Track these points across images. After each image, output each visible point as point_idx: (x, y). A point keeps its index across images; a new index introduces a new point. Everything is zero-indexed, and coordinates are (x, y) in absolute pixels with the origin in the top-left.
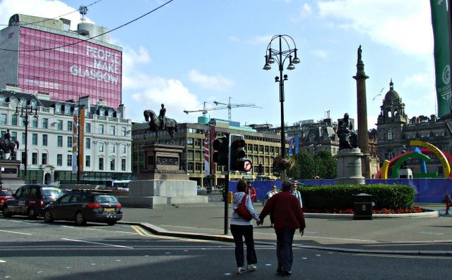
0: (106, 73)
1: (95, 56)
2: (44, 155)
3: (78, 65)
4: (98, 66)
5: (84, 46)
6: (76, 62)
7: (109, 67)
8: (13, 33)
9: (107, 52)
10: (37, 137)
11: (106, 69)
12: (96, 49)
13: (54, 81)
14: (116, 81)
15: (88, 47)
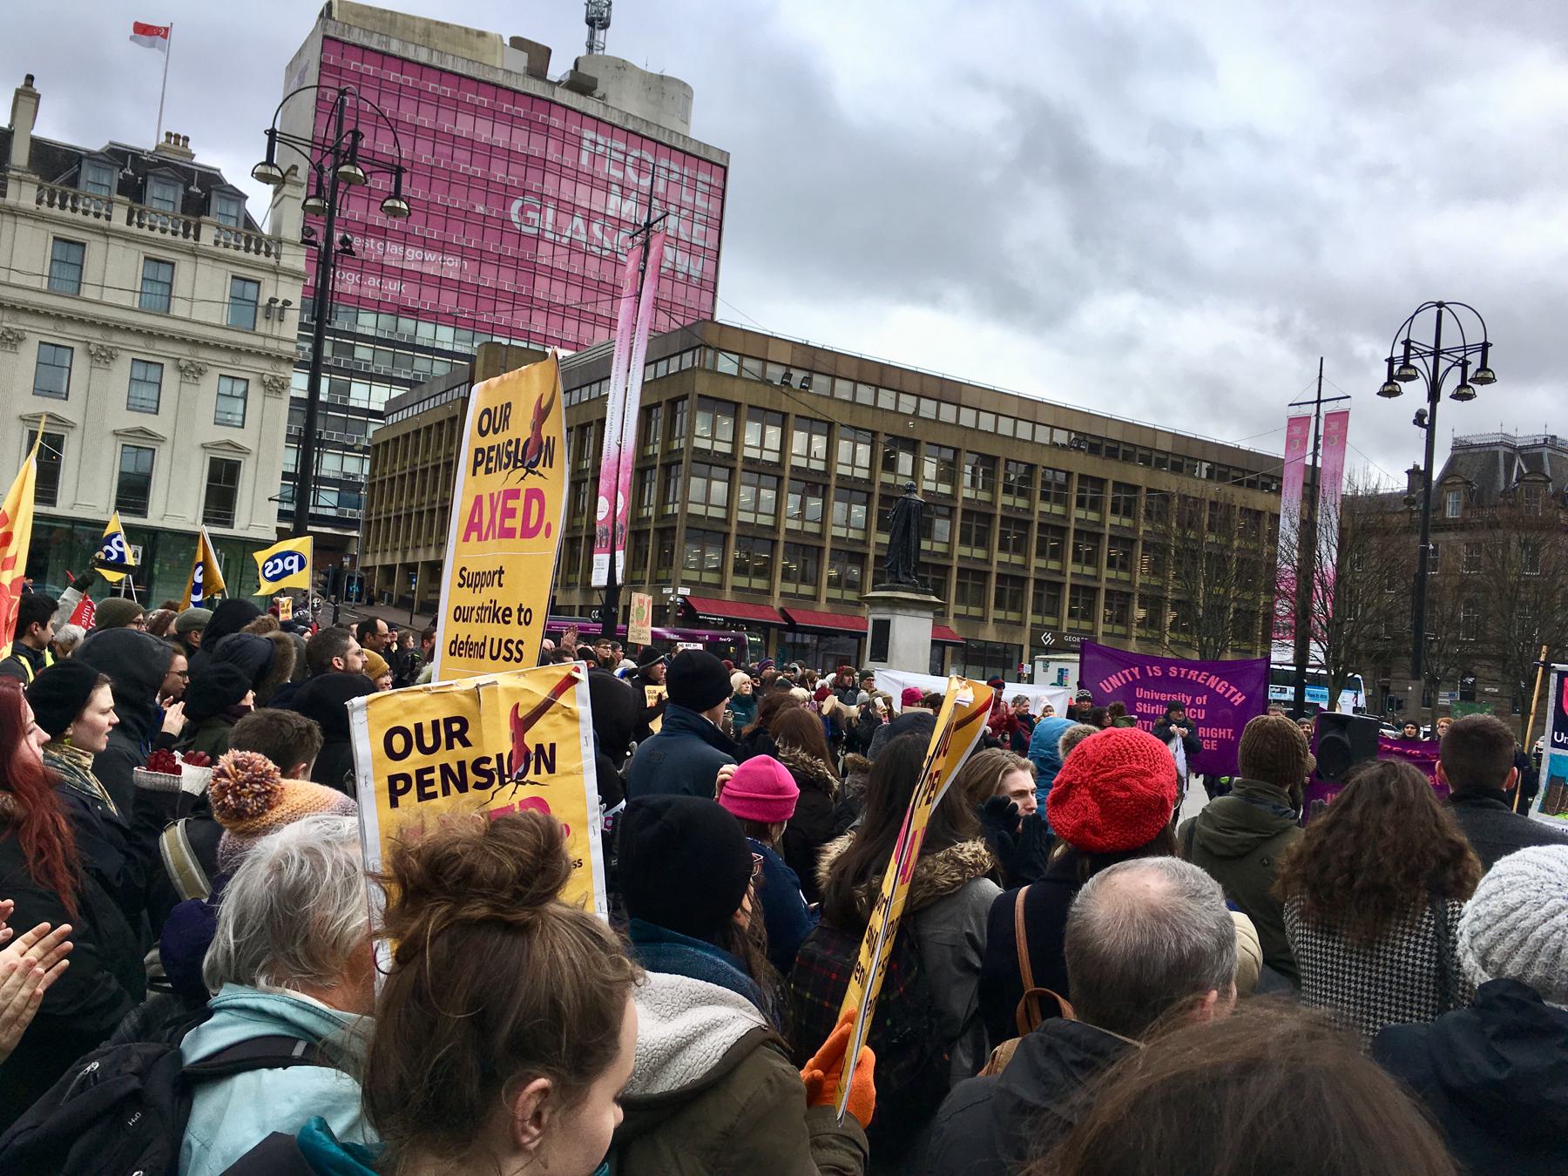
1: (619, 175)
3: (541, 196)
5: (574, 128)
6: (535, 185)
8: (306, 68)
9: (664, 163)
12: (622, 147)
13: (443, 247)
15: (589, 134)
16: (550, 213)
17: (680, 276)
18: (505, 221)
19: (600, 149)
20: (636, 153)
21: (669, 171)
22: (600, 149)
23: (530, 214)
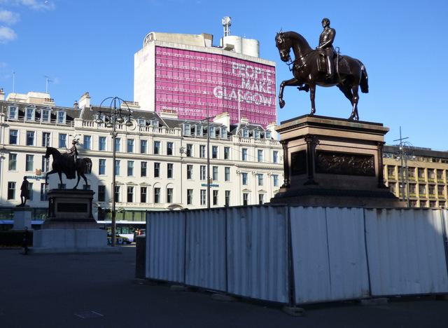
0: (257, 94)
2: (169, 191)
3: (223, 86)
7: (261, 87)
8: (148, 55)
9: (256, 68)
10: (145, 166)
11: (257, 88)
13: (195, 107)
14: (269, 103)
15: (234, 63)
16: (225, 90)
18: (213, 95)
21: (258, 71)
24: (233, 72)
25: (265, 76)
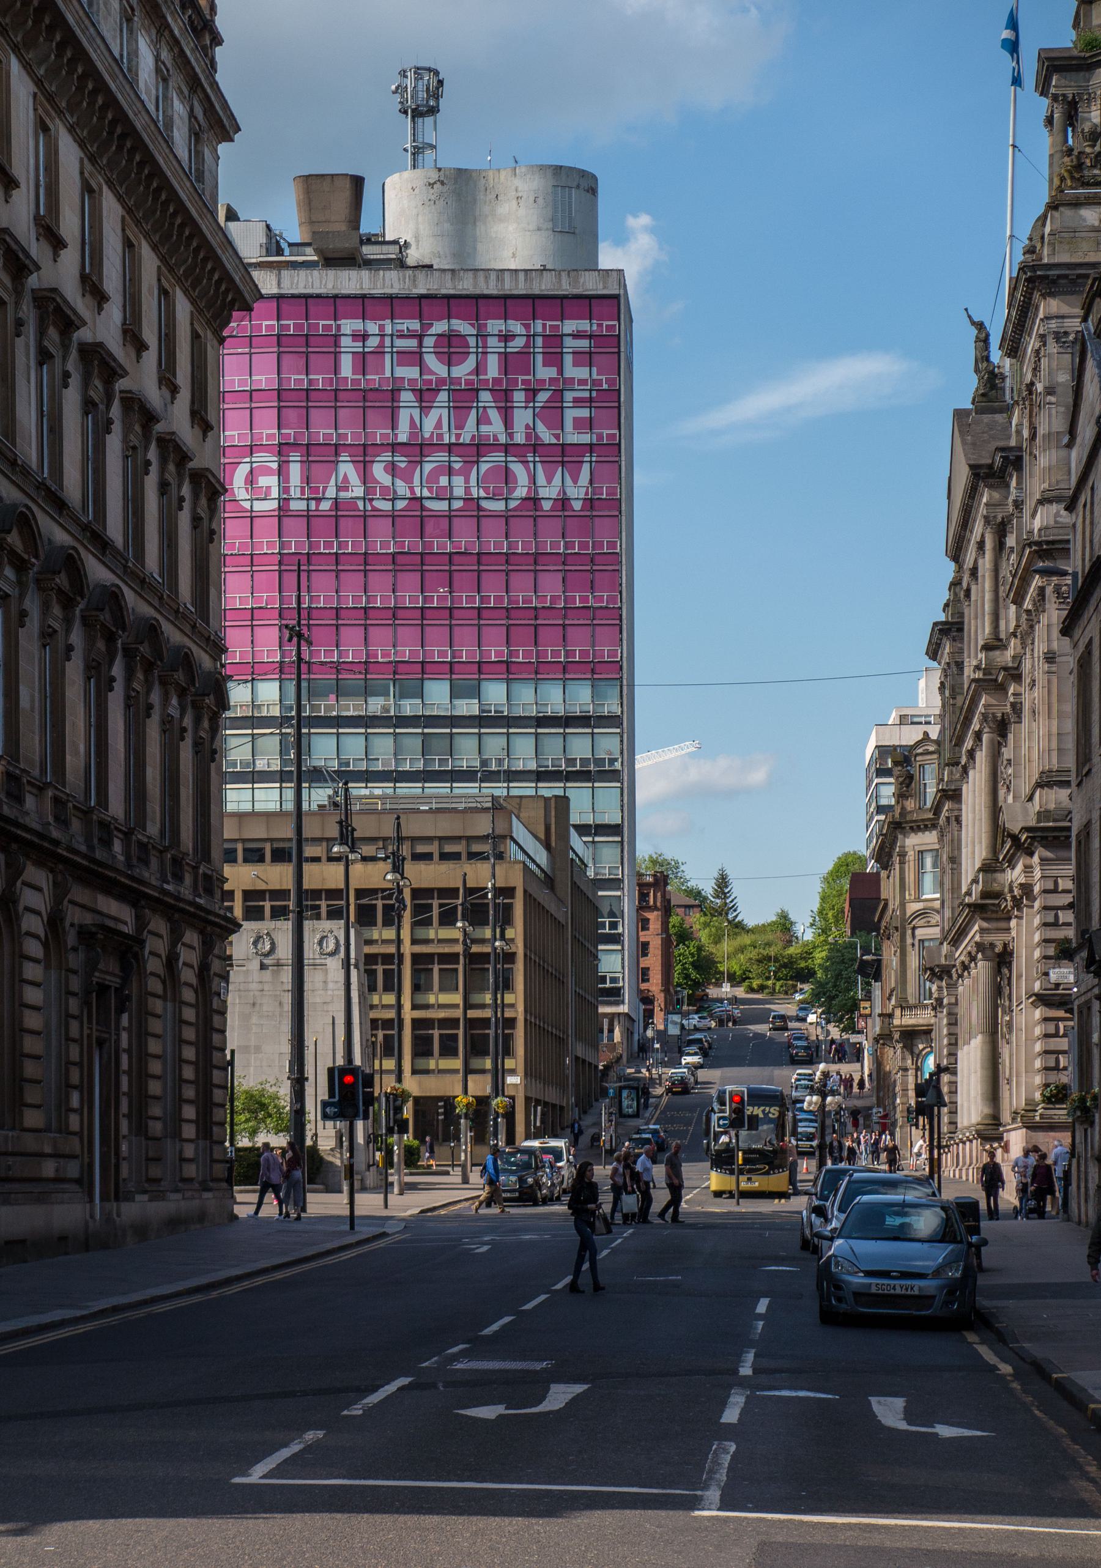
1: (410, 373)
4: (435, 421)
7: (522, 417)
15: (349, 326)
16: (295, 471)
17: (547, 506)
19: (373, 342)
20: (440, 327)
22: (373, 342)
23: (264, 481)
24: (347, 368)
25: (554, 358)
